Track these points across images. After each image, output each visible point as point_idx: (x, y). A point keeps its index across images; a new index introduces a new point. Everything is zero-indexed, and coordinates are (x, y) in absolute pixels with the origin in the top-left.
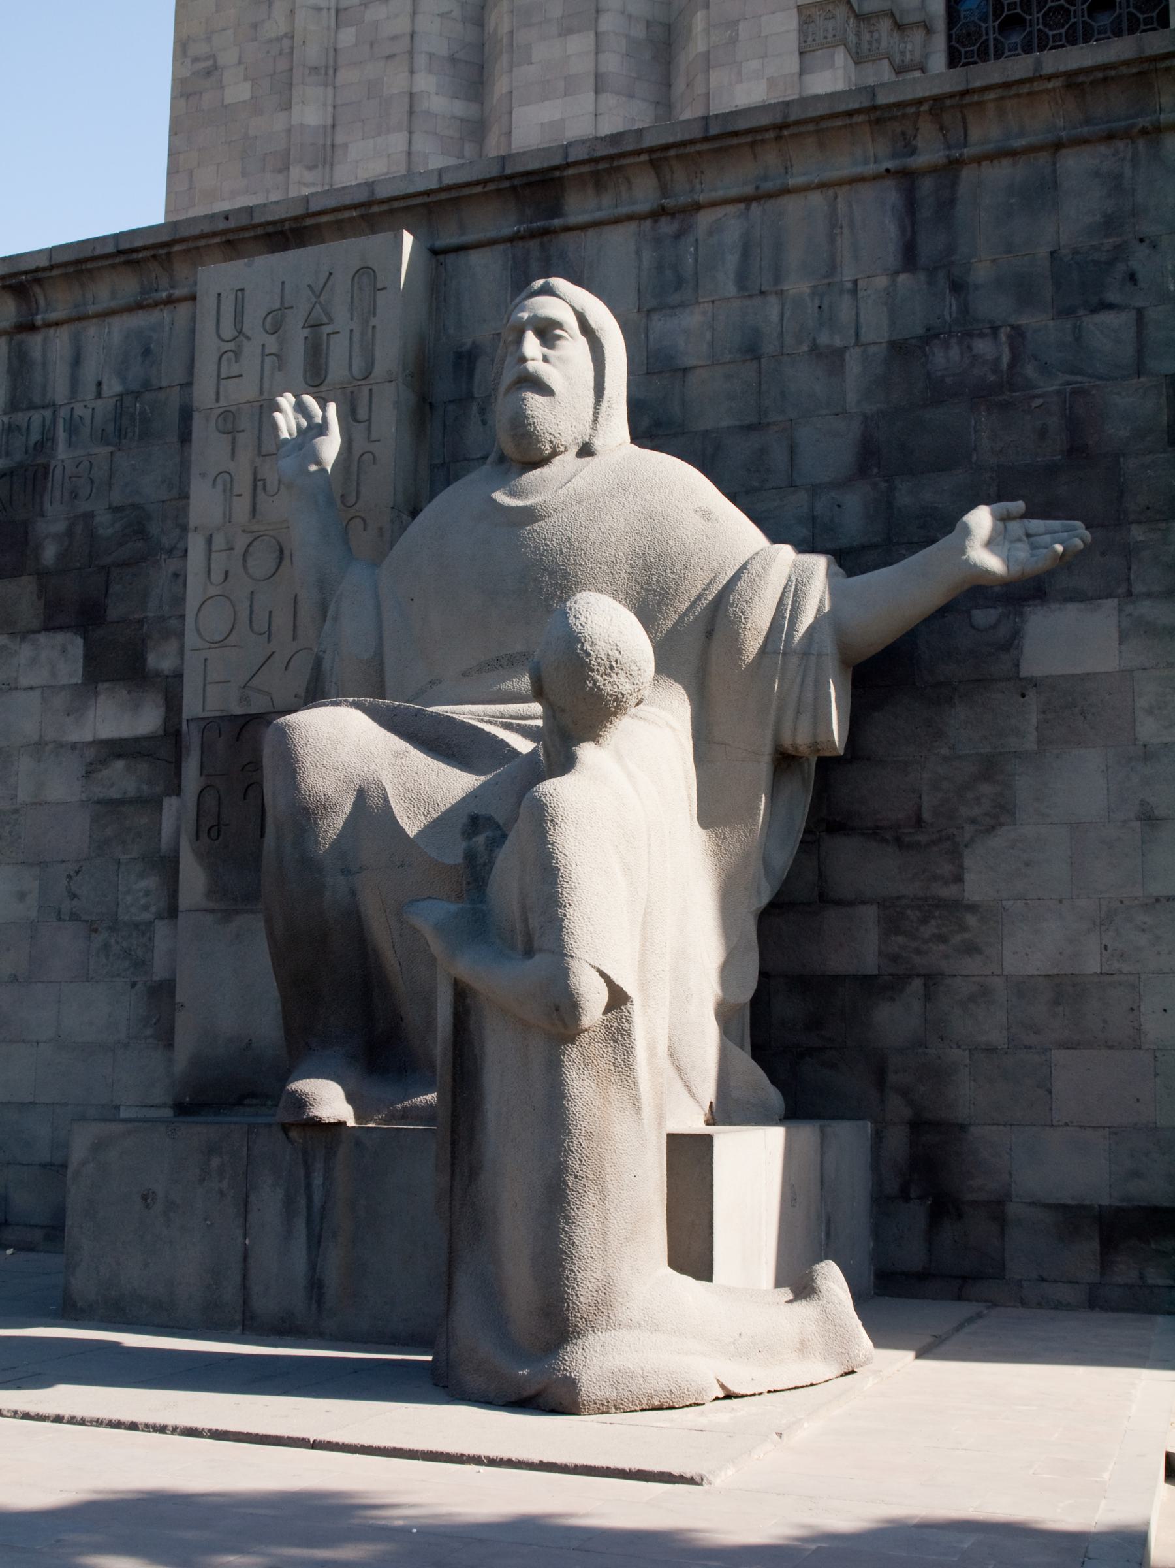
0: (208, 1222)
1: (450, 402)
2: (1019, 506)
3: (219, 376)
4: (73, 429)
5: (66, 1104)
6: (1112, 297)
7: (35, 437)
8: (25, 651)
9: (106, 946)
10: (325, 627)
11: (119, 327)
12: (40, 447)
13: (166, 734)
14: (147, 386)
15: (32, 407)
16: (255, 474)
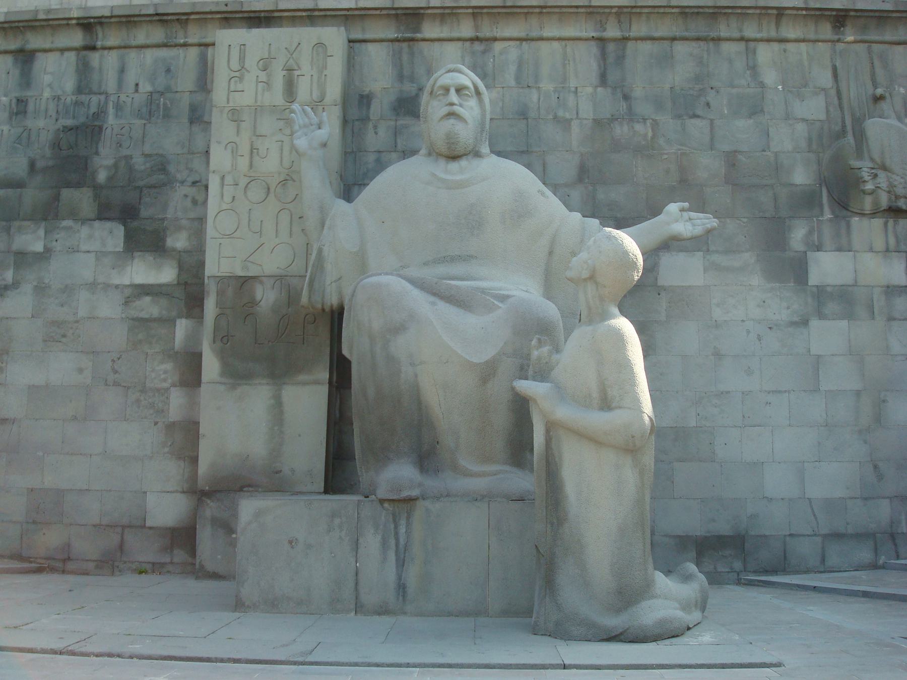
0: (333, 555)
1: (357, 120)
2: (686, 205)
3: (229, 89)
4: (119, 107)
5: (110, 491)
6: (699, 112)
7: (93, 109)
8: (85, 231)
9: (138, 401)
10: (324, 232)
11: (150, 55)
12: (96, 116)
13: (179, 284)
14: (168, 89)
15: (91, 92)
16: (252, 145)
